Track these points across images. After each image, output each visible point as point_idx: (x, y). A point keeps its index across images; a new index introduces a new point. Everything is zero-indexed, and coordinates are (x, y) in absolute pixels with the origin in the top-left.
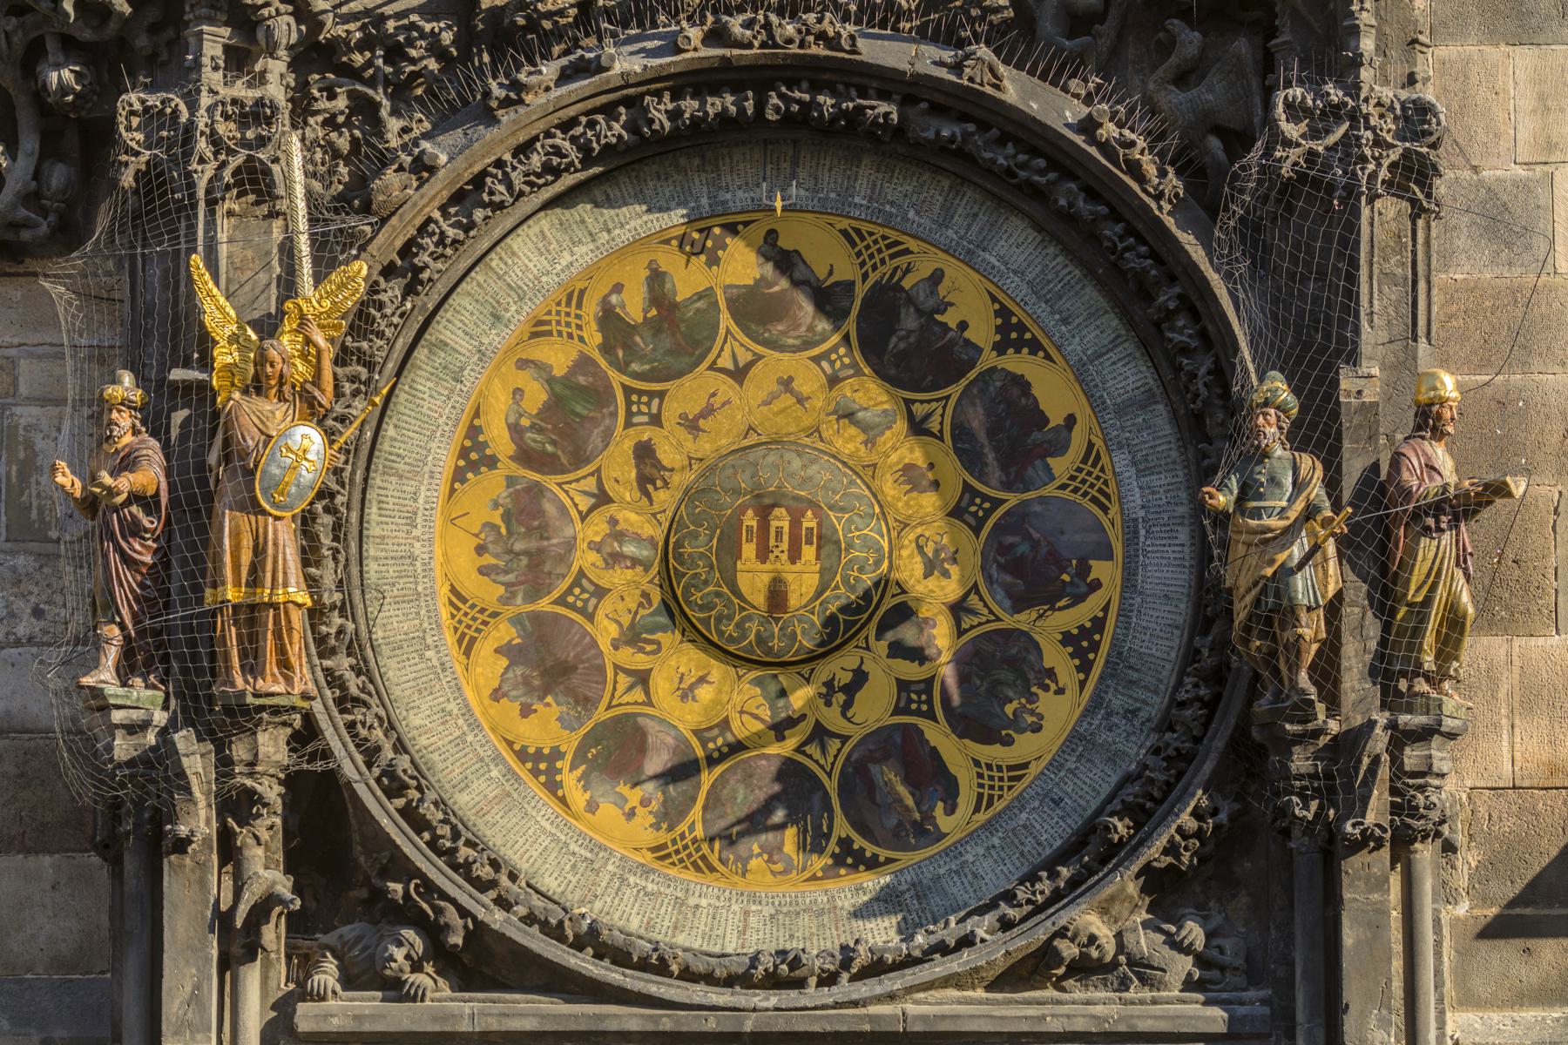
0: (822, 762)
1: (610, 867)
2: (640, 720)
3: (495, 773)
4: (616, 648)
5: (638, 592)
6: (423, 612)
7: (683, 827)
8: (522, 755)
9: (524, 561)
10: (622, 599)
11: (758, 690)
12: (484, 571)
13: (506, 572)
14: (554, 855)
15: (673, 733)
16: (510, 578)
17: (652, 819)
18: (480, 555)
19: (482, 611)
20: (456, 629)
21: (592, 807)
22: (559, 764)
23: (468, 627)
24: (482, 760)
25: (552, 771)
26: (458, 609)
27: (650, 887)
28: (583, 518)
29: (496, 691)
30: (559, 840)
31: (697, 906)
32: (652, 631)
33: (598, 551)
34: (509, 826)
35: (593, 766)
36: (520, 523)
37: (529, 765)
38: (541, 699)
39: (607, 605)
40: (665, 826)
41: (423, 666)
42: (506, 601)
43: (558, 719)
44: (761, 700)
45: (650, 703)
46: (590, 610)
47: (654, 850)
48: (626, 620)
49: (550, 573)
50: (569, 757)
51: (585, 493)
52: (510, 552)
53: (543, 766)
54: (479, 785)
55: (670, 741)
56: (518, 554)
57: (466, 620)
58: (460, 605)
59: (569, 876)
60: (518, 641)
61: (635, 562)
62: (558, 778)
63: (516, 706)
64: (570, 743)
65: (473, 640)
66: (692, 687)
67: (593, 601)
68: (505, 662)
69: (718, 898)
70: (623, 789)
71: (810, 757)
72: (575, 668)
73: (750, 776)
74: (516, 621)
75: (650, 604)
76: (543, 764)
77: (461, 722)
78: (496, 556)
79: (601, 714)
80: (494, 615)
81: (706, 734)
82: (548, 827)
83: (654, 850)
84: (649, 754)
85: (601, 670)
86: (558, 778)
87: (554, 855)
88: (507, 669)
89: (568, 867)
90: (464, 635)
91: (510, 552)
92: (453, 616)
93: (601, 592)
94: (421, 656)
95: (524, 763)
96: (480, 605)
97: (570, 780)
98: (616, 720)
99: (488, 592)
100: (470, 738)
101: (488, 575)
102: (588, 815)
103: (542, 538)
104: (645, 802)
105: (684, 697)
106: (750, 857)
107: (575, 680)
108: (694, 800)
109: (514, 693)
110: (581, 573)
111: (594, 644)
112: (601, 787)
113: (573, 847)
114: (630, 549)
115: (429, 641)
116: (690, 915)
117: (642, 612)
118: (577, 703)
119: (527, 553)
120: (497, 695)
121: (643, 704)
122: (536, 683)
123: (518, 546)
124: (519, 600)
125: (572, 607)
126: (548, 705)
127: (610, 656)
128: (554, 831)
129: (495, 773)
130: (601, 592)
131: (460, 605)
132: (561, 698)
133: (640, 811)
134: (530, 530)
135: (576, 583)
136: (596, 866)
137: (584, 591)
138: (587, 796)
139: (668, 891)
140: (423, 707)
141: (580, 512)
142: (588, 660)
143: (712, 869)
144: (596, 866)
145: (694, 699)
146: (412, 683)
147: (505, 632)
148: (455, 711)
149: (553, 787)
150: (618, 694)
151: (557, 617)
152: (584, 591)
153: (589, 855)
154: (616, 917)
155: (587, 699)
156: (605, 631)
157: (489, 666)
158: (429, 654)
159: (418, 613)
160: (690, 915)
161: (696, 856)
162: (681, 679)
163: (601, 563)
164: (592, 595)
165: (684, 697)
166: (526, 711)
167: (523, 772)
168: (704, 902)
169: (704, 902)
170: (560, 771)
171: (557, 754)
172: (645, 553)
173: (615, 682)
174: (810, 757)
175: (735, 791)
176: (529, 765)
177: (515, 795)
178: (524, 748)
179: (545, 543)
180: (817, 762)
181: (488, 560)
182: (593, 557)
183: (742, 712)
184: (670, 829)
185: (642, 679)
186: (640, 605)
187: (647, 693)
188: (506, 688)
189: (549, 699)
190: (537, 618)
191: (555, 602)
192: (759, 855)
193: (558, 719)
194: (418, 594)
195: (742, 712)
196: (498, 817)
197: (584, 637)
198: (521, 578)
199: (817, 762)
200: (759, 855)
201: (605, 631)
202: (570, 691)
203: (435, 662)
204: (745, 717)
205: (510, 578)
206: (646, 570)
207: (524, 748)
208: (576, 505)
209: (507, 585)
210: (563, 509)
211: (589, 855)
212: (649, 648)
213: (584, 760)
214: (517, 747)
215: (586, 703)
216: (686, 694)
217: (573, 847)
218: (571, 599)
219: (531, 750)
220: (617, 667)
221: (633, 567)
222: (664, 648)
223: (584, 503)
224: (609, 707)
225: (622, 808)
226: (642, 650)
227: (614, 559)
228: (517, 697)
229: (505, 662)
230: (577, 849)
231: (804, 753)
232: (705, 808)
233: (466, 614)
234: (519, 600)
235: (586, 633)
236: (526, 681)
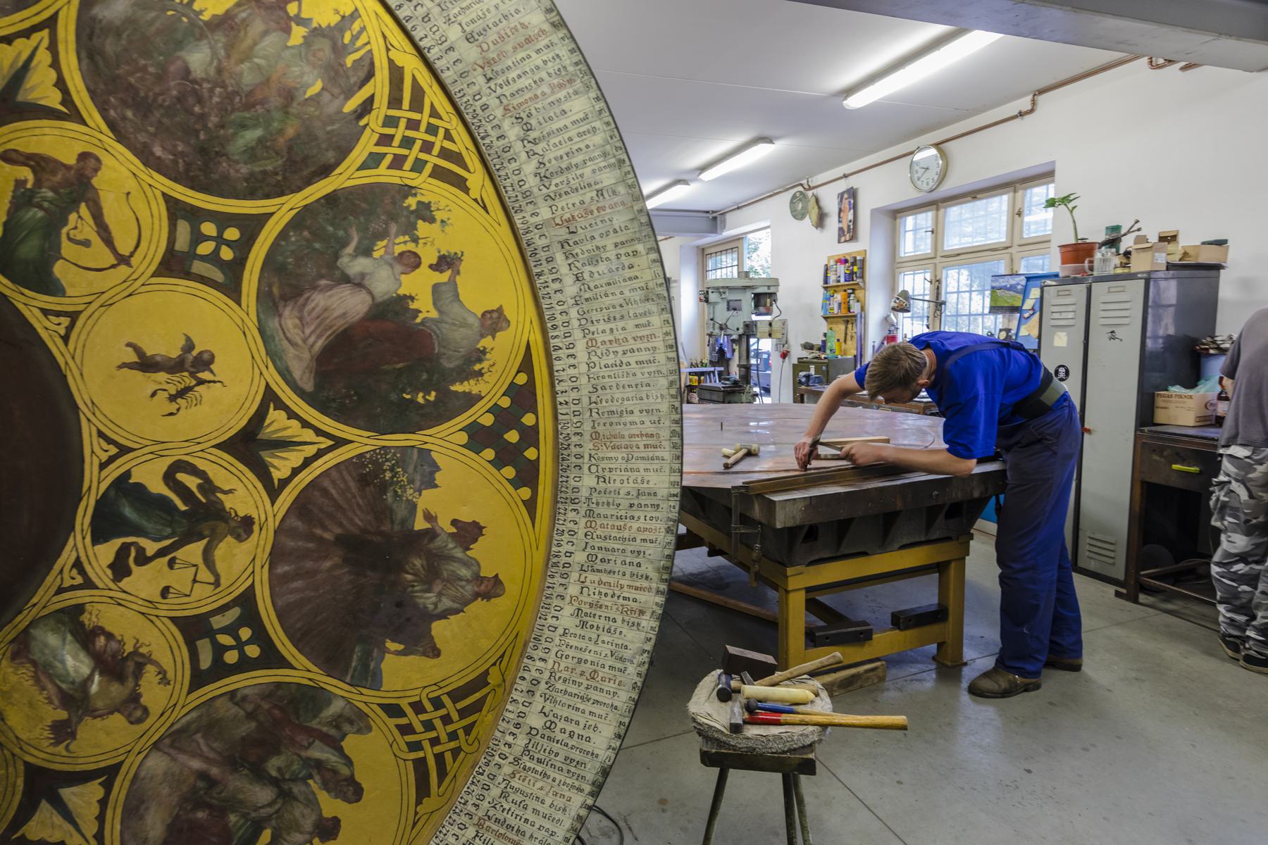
0: (43, 57)
1: (545, 213)
2: (309, 387)
3: (589, 481)
4: (248, 522)
5: (125, 583)
6: (495, 792)
7: (384, 174)
8: (527, 476)
9: (274, 765)
10: (165, 592)
11: (59, 269)
12: (351, 790)
13: (319, 765)
14: (607, 301)
15: (273, 323)
16: (319, 752)
17: (423, 228)
18: (336, 822)
19: (406, 730)
20: (468, 730)
21: (494, 321)
22: (488, 420)
23: (446, 720)
24: (590, 513)
25: (506, 419)
26: (440, 758)
27: (513, 132)
28: (108, 774)
29: (487, 596)
30: (583, 315)
31: (470, 38)
32: (162, 502)
33: (135, 698)
34: (630, 393)
35: (439, 378)
36: (227, 834)
37: (531, 454)
38: (431, 534)
39: (202, 599)
40: (411, 202)
41: (559, 710)
42: (358, 721)
43: (432, 484)
44: (67, 248)
45: (270, 398)
46: (235, 613)
47: (460, 183)
48: (193, 551)
49: (250, 716)
50: (464, 419)
51: (68, 815)
52: (285, 796)
53: (513, 436)
54: (623, 483)
55: (289, 319)
56: (275, 782)
57: (442, 731)
58: (431, 763)
59: (612, 254)
60: (392, 646)
61: (86, 637)
62: (506, 402)
63: (476, 550)
64: (444, 441)
65: (456, 695)
66: (175, 366)
67: (218, 622)
68: (438, 628)
69: (426, 18)
70: (425, 307)
71: (61, 84)
72: (340, 541)
73: (202, 150)
74: (369, 677)
75: (124, 549)
76: (510, 441)
77: (573, 590)
78: (312, 802)
79: (361, 442)
80: (393, 710)
81: (219, 276)
82: (581, 346)
83: (460, 183)
84: (340, 325)
85: (301, 507)
86: (506, 402)
87: (607, 301)
88: (444, 615)
89: (602, 267)
90: (463, 713)
91: (285, 796)
92: (456, 752)
93: (193, 628)
94: (550, 727)
95: (535, 464)
96: (402, 741)
97: (490, 388)
98: (342, 414)
99: (375, 755)
100: (580, 557)
101: (351, 781)
102: (508, 313)
103: (211, 782)
104: (411, 262)
105: (205, 362)
106: (317, 32)
107: (358, 520)
108: (331, 199)
109: (464, 572)
110: (199, 679)
111: (277, 555)
112: (459, 338)
113: (571, 289)
114: (75, 663)
115: (521, 741)
116: (492, 36)
117: (151, 547)
118: (384, 487)
119: (259, 774)
120: (491, 588)
121: (281, 405)
122: (418, 563)
123: (263, 795)
124: (336, 707)
125: (260, 635)
126: (429, 517)
127: (269, 514)
128: (578, 334)
129: (589, 481)
130: (193, 628)
131: (431, 763)
132: (401, 512)
133: (429, 256)
134: (220, 811)
135: (220, 670)
136: (562, 233)
137: (219, 650)
138: (486, 342)
139: (493, 102)
140: (606, 649)
141: (108, 786)
142: (311, 537)
143: (396, 74)
144: (562, 233)
145: (189, 346)
146: (594, 695)
147: (402, 673)
148: (568, 610)
149: (523, 397)
150: (310, 451)
151: (298, 640)
152: (219, 650)
153: (559, 257)
154: (598, 139)
155: (364, 481)
156: (242, 562)
157: (462, 638)
158: (536, 721)
159: (504, 795)
160: (492, 36)
161: (405, 114)
162: (182, 393)
163: (150, 672)
164: (211, 634)
165: (205, 362)
166: (469, 532)
167: (543, 454)
168: (454, 34)
169: (454, 34)
170: (495, 410)
171: (478, 438)
172: (53, 640)
173: (296, 472)
174: (61, 84)
175: (252, 153)
176: (531, 454)
177: (587, 427)
178: (517, 483)
179: (215, 771)
180: (55, 64)
181: (330, 806)
182: (153, 693)
183: (124, 260)
184: (408, 190)
185: (248, 445)
186: (143, 559)
187: (259, 417)
188: (469, 589)
189: (420, 524)
190: (333, 661)
191: (284, 663)
192: (301, 21)
193: (432, 484)
194: (479, 825)
195: (124, 260)
196: (636, 417)
197: (285, 579)
198: (302, 739)
199: (55, 64)
200: (301, 21)
201: (242, 562)
202: (381, 512)
203: (538, 702)
204: (124, 249)
205: (319, 752)
206: (79, 609)
207: (517, 483)
208: (103, 803)
209: (335, 744)
210: (133, 810)
211: (559, 257)
212: (192, 482)
213: (445, 394)
214: (525, 493)
215: (368, 474)
216: (193, 365)
217: (571, 289)
218: (253, 651)
219: (509, 472)
220: (274, 491)
221: (99, 631)
222: (163, 465)
223: (84, 799)
224: (340, 442)
225: (452, 283)
226: (208, 486)
227: (120, 665)
228: (466, 564)
229: (438, 628)
230: (569, 280)
231: (67, 99)
232: (325, 171)
233: (435, 742)
234: (336, 707)
235: (276, 582)
236: (432, 575)
